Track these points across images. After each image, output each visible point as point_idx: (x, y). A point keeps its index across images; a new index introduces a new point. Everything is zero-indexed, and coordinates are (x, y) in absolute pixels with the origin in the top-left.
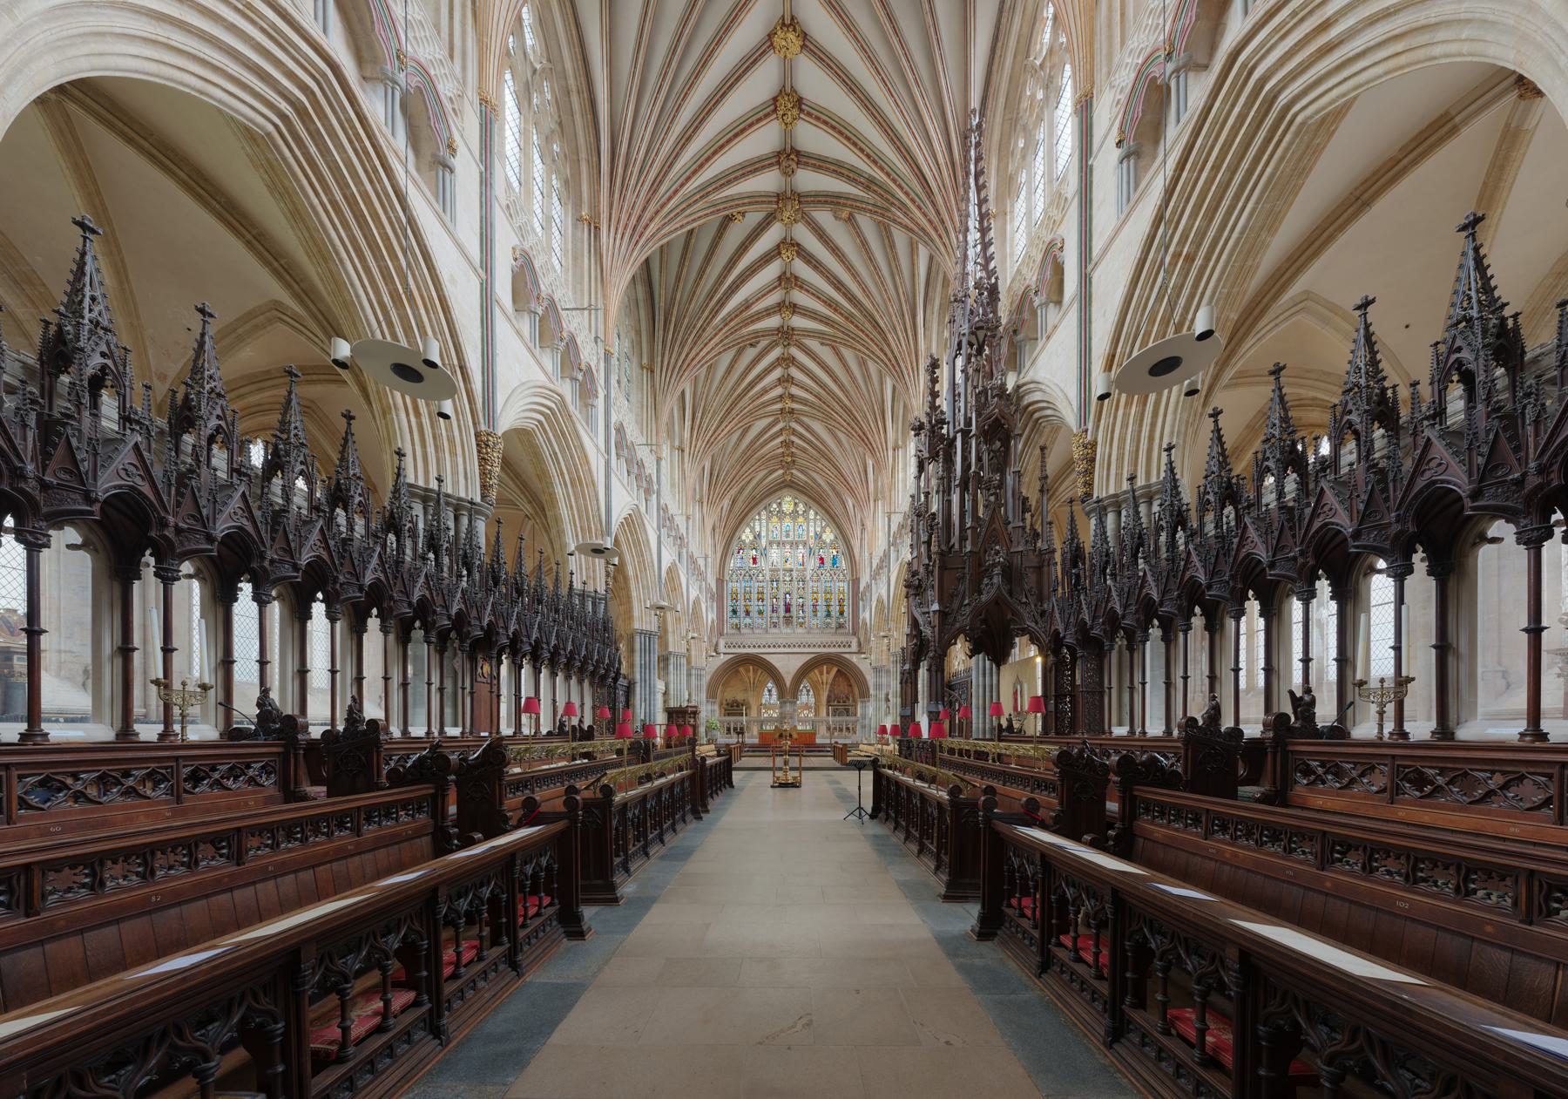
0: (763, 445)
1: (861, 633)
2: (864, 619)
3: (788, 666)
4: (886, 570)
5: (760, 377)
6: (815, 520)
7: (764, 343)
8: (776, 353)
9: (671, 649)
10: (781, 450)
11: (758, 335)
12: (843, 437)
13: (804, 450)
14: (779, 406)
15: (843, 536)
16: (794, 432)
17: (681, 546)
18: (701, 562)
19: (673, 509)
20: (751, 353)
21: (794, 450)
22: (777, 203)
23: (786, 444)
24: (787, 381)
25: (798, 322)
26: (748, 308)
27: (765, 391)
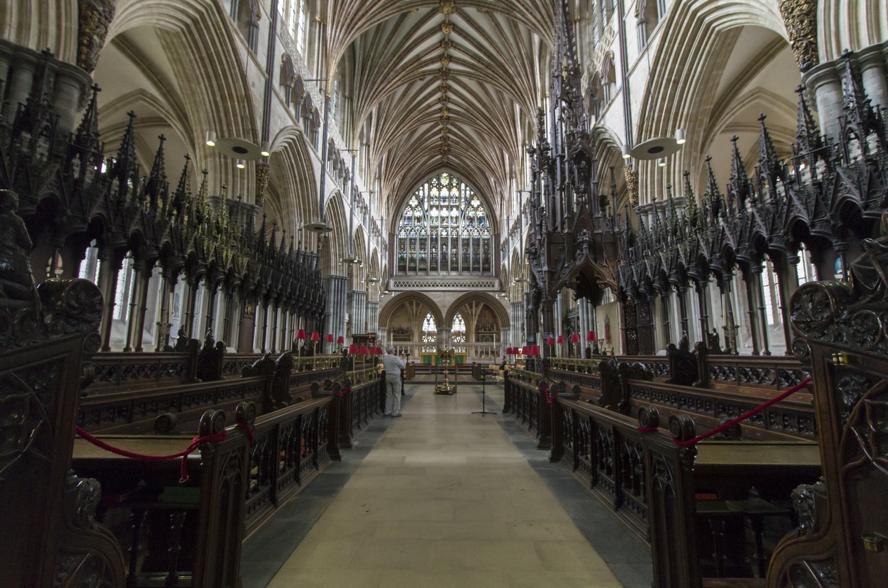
0: (426, 140)
1: (502, 276)
2: (504, 265)
3: (444, 299)
4: (519, 230)
5: (426, 98)
6: (466, 190)
7: (429, 78)
8: (438, 83)
9: (354, 289)
10: (440, 143)
11: (424, 74)
12: (486, 136)
13: (457, 143)
14: (439, 115)
15: (488, 204)
16: (450, 131)
17: (365, 214)
18: (379, 223)
19: (362, 188)
20: (419, 84)
21: (449, 142)
22: (440, 3)
23: (445, 139)
24: (446, 100)
25: (453, 66)
26: (419, 59)
27: (429, 106)
